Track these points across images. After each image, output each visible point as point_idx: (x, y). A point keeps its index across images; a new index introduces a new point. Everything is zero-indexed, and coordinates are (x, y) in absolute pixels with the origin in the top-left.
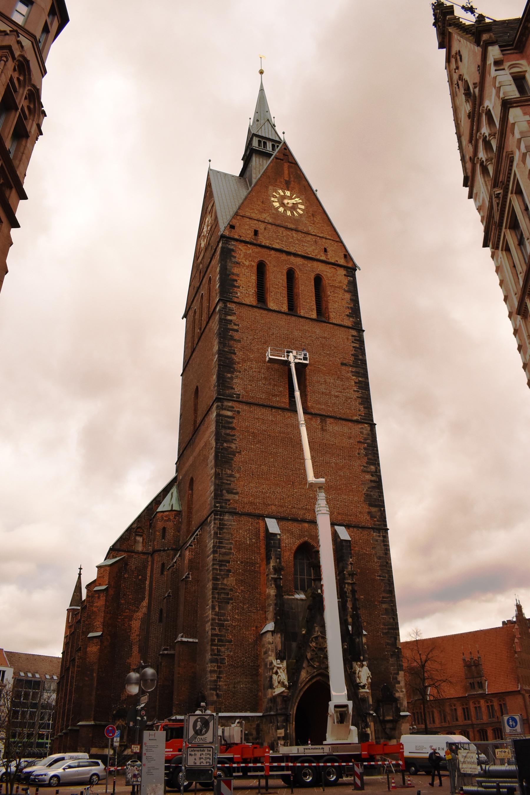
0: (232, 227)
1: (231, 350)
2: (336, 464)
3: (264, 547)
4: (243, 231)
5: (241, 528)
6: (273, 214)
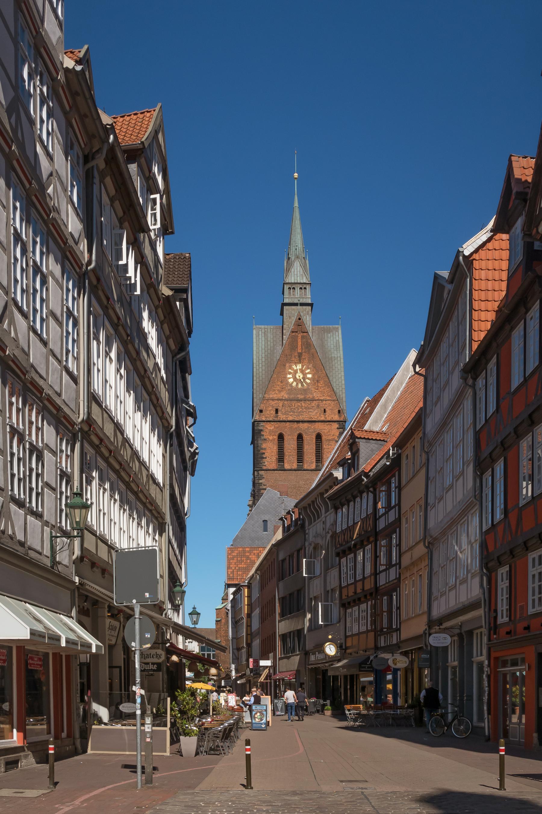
0: (261, 411)
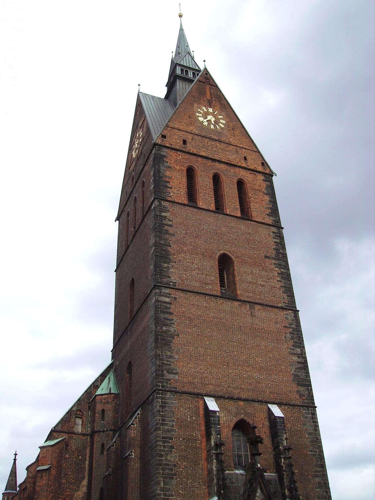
0: (164, 137)
1: (167, 242)
2: (266, 347)
3: (203, 424)
4: (174, 140)
5: (181, 407)
6: (199, 127)
